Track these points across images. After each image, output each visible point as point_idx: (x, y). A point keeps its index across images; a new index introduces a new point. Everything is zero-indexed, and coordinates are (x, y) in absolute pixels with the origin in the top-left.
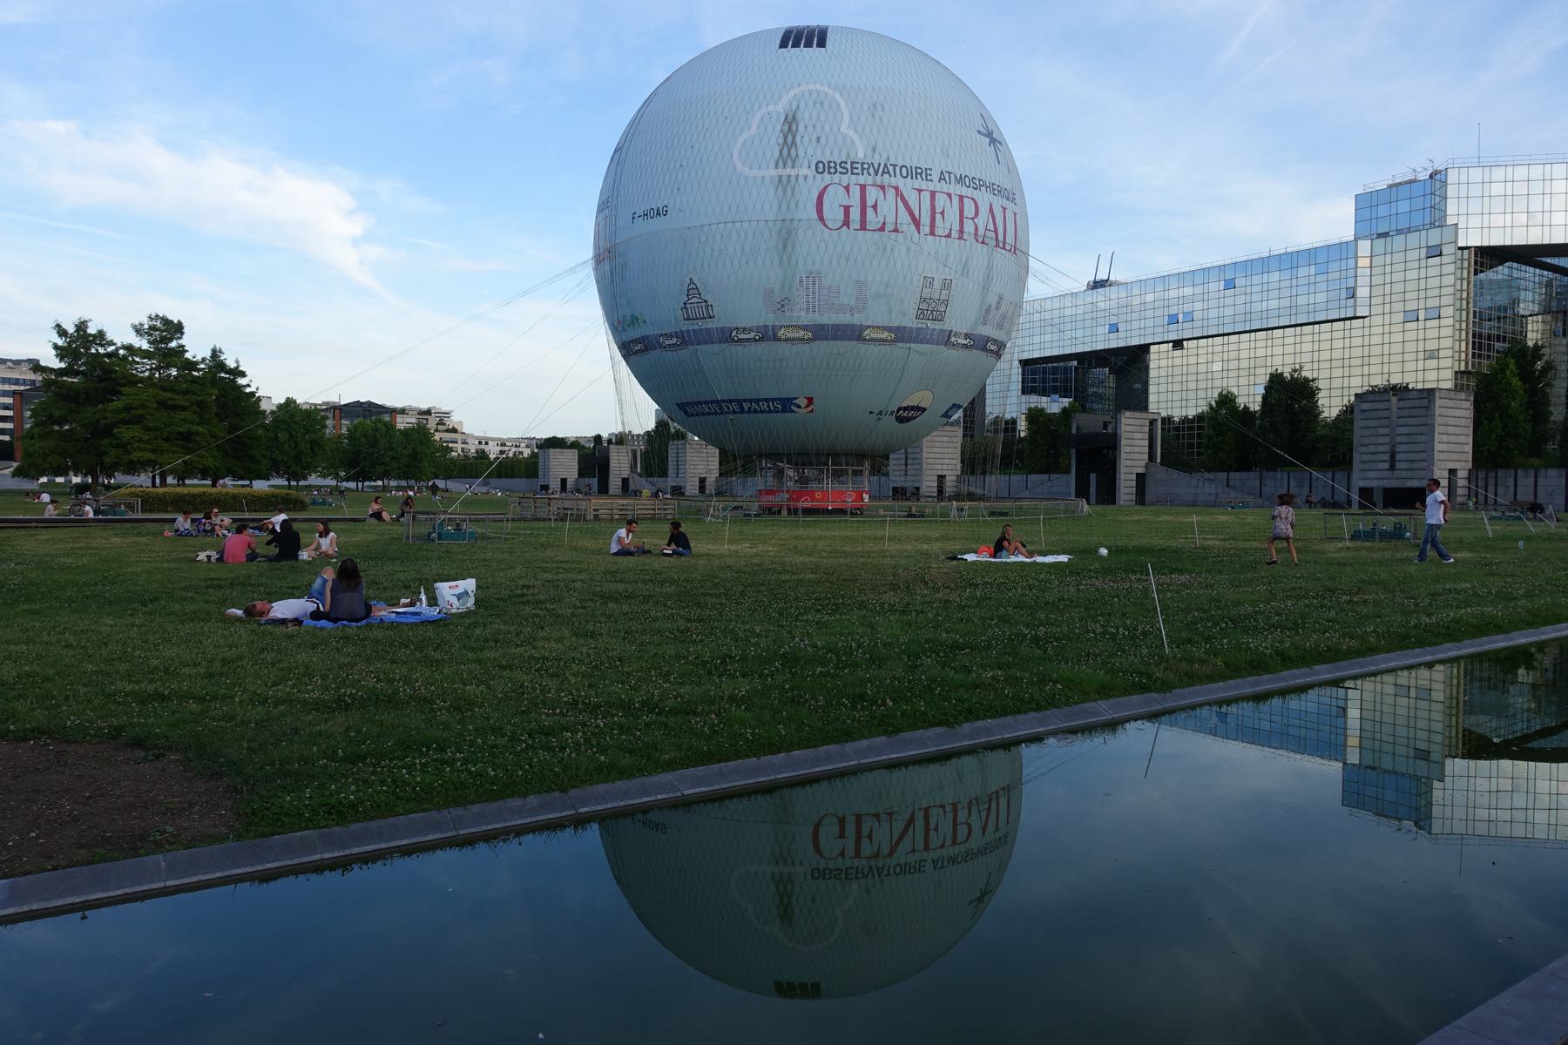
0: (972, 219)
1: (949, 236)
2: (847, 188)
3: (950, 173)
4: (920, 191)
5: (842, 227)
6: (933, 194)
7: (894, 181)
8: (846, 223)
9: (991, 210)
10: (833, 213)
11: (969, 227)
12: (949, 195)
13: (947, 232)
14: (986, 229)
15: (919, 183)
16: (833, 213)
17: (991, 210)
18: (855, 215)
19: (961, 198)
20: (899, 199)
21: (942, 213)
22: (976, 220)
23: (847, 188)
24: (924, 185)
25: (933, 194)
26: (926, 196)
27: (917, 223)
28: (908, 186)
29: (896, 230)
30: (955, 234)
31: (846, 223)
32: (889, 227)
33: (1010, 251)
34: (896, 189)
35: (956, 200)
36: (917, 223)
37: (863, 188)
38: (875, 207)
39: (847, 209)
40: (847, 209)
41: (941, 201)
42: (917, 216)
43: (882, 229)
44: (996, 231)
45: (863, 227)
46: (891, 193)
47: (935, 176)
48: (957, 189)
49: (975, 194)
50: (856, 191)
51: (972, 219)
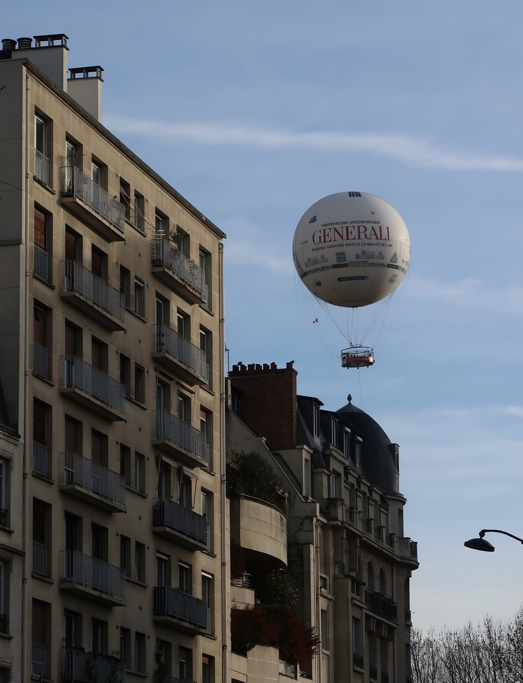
0: (364, 232)
1: (354, 239)
2: (320, 231)
4: (342, 227)
6: (347, 228)
7: (334, 226)
8: (320, 242)
10: (317, 240)
11: (362, 235)
12: (354, 227)
14: (371, 235)
15: (342, 226)
16: (317, 240)
17: (373, 228)
18: (322, 240)
19: (359, 227)
20: (335, 232)
21: (351, 233)
23: (320, 231)
24: (342, 226)
25: (347, 228)
26: (345, 229)
27: (342, 237)
28: (338, 227)
29: (335, 240)
30: (357, 237)
31: (320, 242)
32: (333, 239)
33: (385, 239)
34: (335, 230)
35: (356, 228)
36: (342, 237)
37: (324, 230)
38: (328, 235)
39: (320, 237)
40: (320, 237)
41: (350, 229)
42: (342, 235)
43: (330, 241)
44: (376, 234)
45: (325, 241)
46: (333, 230)
47: (349, 222)
48: (356, 225)
49: (363, 224)
50: (322, 231)
51: (364, 232)
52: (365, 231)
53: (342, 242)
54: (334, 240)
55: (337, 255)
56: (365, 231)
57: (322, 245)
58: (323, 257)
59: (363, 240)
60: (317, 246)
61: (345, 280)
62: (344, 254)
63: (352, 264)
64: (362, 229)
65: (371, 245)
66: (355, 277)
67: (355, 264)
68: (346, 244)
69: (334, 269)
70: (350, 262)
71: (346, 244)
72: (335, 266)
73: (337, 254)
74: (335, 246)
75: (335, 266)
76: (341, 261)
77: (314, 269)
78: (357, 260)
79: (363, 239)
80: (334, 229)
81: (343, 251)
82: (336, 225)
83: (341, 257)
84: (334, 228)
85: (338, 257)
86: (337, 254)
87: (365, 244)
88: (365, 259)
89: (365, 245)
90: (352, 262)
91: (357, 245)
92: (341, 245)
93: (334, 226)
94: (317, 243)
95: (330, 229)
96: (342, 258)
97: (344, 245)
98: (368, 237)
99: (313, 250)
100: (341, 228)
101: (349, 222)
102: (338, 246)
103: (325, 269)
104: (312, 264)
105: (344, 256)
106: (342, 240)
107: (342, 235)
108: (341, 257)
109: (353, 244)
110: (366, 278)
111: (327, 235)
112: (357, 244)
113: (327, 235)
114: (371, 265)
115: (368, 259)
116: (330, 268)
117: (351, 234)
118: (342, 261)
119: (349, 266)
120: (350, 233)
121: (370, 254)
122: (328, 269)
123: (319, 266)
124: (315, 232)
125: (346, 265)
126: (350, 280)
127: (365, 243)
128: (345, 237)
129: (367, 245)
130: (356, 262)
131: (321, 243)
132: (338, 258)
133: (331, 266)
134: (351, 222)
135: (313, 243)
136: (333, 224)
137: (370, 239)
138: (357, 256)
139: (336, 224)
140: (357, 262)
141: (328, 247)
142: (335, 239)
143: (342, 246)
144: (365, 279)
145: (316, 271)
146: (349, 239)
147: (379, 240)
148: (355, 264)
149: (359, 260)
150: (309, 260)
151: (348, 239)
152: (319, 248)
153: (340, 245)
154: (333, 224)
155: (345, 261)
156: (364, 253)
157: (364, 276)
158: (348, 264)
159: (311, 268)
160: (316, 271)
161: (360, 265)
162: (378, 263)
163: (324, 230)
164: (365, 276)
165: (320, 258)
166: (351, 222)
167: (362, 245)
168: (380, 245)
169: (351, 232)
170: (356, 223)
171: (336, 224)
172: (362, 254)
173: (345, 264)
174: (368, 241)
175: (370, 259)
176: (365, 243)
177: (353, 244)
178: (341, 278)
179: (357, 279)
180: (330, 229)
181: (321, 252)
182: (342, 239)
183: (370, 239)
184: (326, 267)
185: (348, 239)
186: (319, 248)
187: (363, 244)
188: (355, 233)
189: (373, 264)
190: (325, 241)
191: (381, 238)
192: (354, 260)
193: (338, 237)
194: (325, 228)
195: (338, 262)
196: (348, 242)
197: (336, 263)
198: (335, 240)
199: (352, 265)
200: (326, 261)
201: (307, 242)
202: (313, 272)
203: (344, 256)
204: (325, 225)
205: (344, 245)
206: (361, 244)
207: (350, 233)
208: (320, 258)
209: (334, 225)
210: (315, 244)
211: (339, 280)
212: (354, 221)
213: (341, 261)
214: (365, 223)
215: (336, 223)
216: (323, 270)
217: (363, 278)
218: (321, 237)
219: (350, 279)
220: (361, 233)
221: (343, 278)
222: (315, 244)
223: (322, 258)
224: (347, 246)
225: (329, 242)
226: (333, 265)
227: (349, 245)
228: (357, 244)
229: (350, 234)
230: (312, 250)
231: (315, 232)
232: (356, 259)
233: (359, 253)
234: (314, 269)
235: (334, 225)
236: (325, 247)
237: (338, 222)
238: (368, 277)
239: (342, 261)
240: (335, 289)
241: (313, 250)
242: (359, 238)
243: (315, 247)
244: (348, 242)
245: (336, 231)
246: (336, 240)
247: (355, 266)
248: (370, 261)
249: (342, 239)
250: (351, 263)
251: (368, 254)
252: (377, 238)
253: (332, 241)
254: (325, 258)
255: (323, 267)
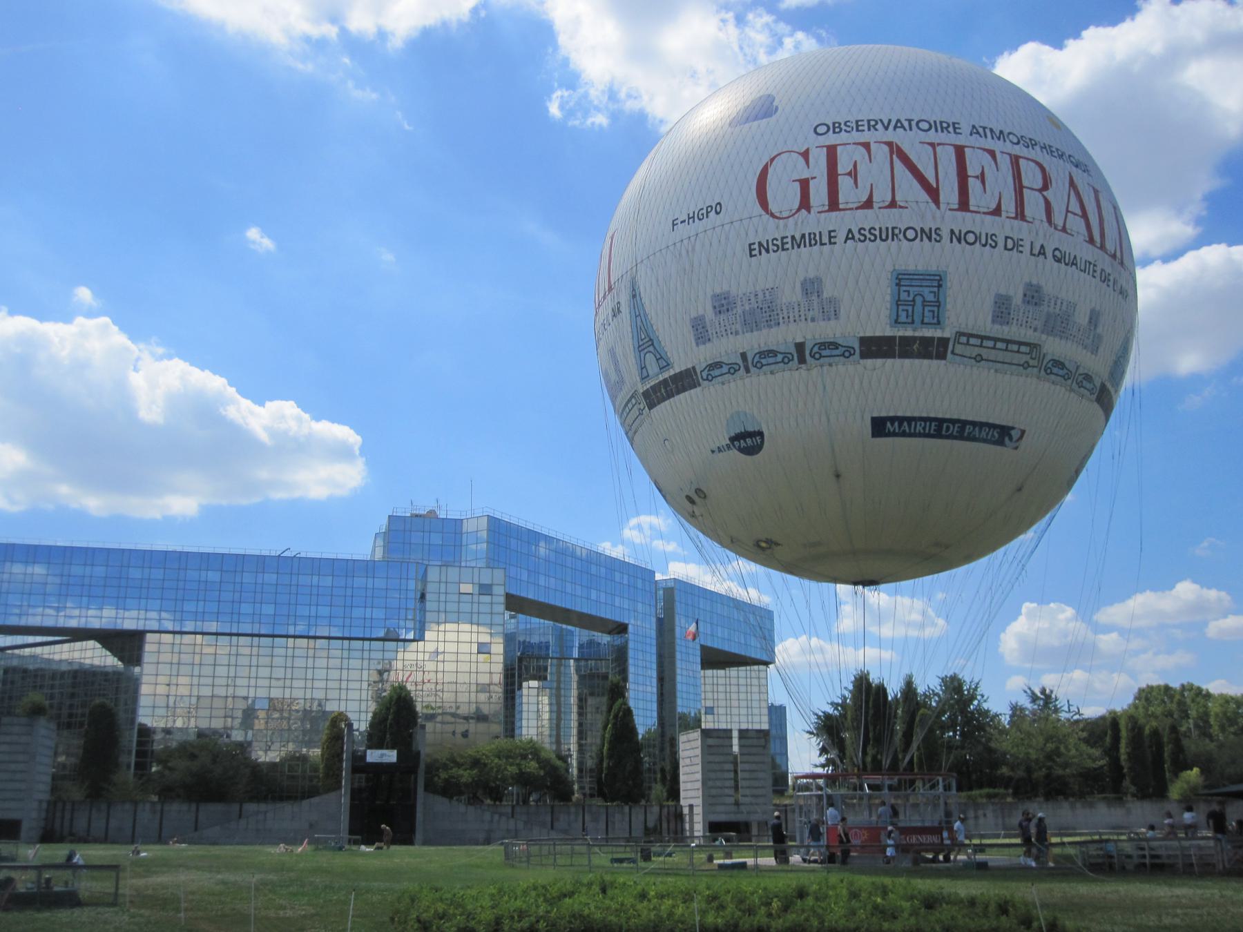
0: (1040, 191)
1: (997, 211)
2: (805, 155)
3: (984, 128)
5: (799, 210)
6: (960, 152)
7: (890, 135)
8: (805, 204)
9: (1072, 184)
10: (783, 195)
11: (1034, 205)
13: (993, 206)
14: (1068, 211)
16: (783, 195)
17: (1072, 184)
19: (1015, 161)
20: (894, 156)
22: (1045, 193)
23: (805, 155)
25: (960, 152)
27: (933, 193)
28: (909, 142)
29: (893, 204)
30: (1009, 206)
31: (805, 204)
35: (1005, 162)
36: (933, 193)
37: (832, 151)
38: (853, 174)
42: (935, 186)
43: (868, 204)
44: (1085, 215)
45: (834, 205)
46: (881, 153)
47: (965, 128)
51: (1040, 191)
52: (1046, 186)
53: (934, 218)
54: (887, 204)
55: (898, 285)
56: (1046, 186)
57: (812, 223)
58: (811, 287)
59: (1034, 231)
60: (786, 226)
61: (910, 435)
62: (940, 286)
63: (968, 343)
64: (1031, 177)
65: (1066, 264)
66: (964, 423)
67: (984, 353)
68: (952, 232)
69: (869, 362)
70: (960, 334)
71: (952, 232)
72: (874, 348)
73: (901, 279)
74: (889, 234)
75: (874, 348)
76: (913, 322)
77: (744, 356)
78: (997, 327)
79: (1037, 223)
80: (886, 149)
81: (933, 268)
82: (900, 130)
83: (919, 300)
84: (890, 144)
85: (904, 296)
86: (901, 279)
87: (1042, 252)
88: (1035, 330)
89: (1044, 254)
90: (970, 336)
91: (1006, 248)
92: (929, 235)
93: (890, 135)
94: (785, 214)
95: (866, 146)
96: (924, 306)
97: (945, 234)
98: (1058, 219)
99: (757, 249)
100: (930, 149)
101: (965, 128)
102: (910, 234)
103: (813, 357)
104: (738, 327)
105: (936, 295)
106: (933, 206)
107: (935, 186)
108: (919, 300)
109: (989, 241)
110: (1011, 439)
111: (849, 174)
112: (1010, 245)
113: (849, 174)
114: (1051, 373)
115: (1044, 337)
116: (848, 353)
117: (978, 183)
118: (922, 323)
119: (953, 352)
120: (977, 177)
121: (1057, 311)
122: (831, 360)
123: (781, 337)
124: (772, 160)
125: (934, 349)
126: (938, 435)
127: (1042, 246)
128: (949, 193)
129: (1054, 256)
130: (989, 338)
131: (808, 209)
132: (898, 303)
133: (857, 346)
134: (974, 127)
135: (758, 209)
136: (879, 126)
137: (1064, 230)
138: (1002, 310)
139: (898, 125)
140: (996, 340)
141: (850, 236)
142: (897, 198)
143: (930, 239)
144: (1007, 439)
145: (748, 363)
146: (972, 208)
147: (1096, 250)
148: (984, 353)
149: (1006, 328)
150: (723, 304)
151: (964, 205)
152: (793, 238)
153: (922, 230)
154: (879, 126)
155: (939, 323)
156: (1033, 295)
157: (1010, 424)
158: (948, 339)
159: (726, 347)
160: (748, 363)
161: (1008, 357)
162: (1078, 368)
163: (832, 151)
164: (1013, 428)
165: (790, 295)
166: (974, 127)
167: (1032, 254)
168: (1098, 274)
169: (978, 173)
170: (999, 139)
171: (895, 127)
172: (1024, 302)
173: (932, 339)
174: (1054, 240)
175: (1051, 338)
176: (1042, 246)
177: (989, 241)
178: (893, 419)
179: (974, 439)
180: (866, 146)
181: (807, 261)
182: (936, 201)
183: (1064, 230)
184: (824, 345)
185: (964, 205)
186: (793, 238)
187: (1036, 251)
188: (1000, 182)
189: (1057, 368)
190: (834, 205)
191: (1102, 247)
192: (982, 322)
193: (909, 189)
194: (831, 139)
195: (896, 322)
196: (963, 222)
197: (883, 328)
198: (893, 204)
199: (969, 351)
200: (831, 310)
201: (717, 213)
202: (733, 370)
203: (936, 295)
204: (836, 128)
205: (945, 234)
206: (1027, 249)
207: (977, 177)
208: (790, 295)
209: (886, 128)
210: (772, 215)
211: (880, 427)
212: (991, 130)
213: (913, 322)
214: (1037, 148)
215: (898, 121)
216: (802, 360)
217: (1002, 434)
218: (812, 183)
219: (940, 428)
220: (1025, 190)
221: (901, 420)
222: (772, 215)
223: (806, 292)
224: (959, 241)
225: (857, 208)
226: (864, 341)
227: (971, 238)
228: (1010, 245)
229: (974, 185)
230: (751, 250)
231: (772, 160)
232: (993, 322)
233: (1011, 293)
234: (744, 356)
235: (886, 128)
236: (830, 237)
237: (910, 121)
238: (1023, 432)
239: (922, 323)
240: (838, 476)
241: (757, 249)
242: (1020, 215)
243: (770, 230)
244: (963, 222)
245: (898, 156)
246: (902, 204)
247: (979, 359)
248: (1054, 347)
249: (936, 201)
250: (964, 339)
251: (1051, 310)
252: (1091, 240)
253: (876, 205)
254: (826, 295)
255: (800, 347)
